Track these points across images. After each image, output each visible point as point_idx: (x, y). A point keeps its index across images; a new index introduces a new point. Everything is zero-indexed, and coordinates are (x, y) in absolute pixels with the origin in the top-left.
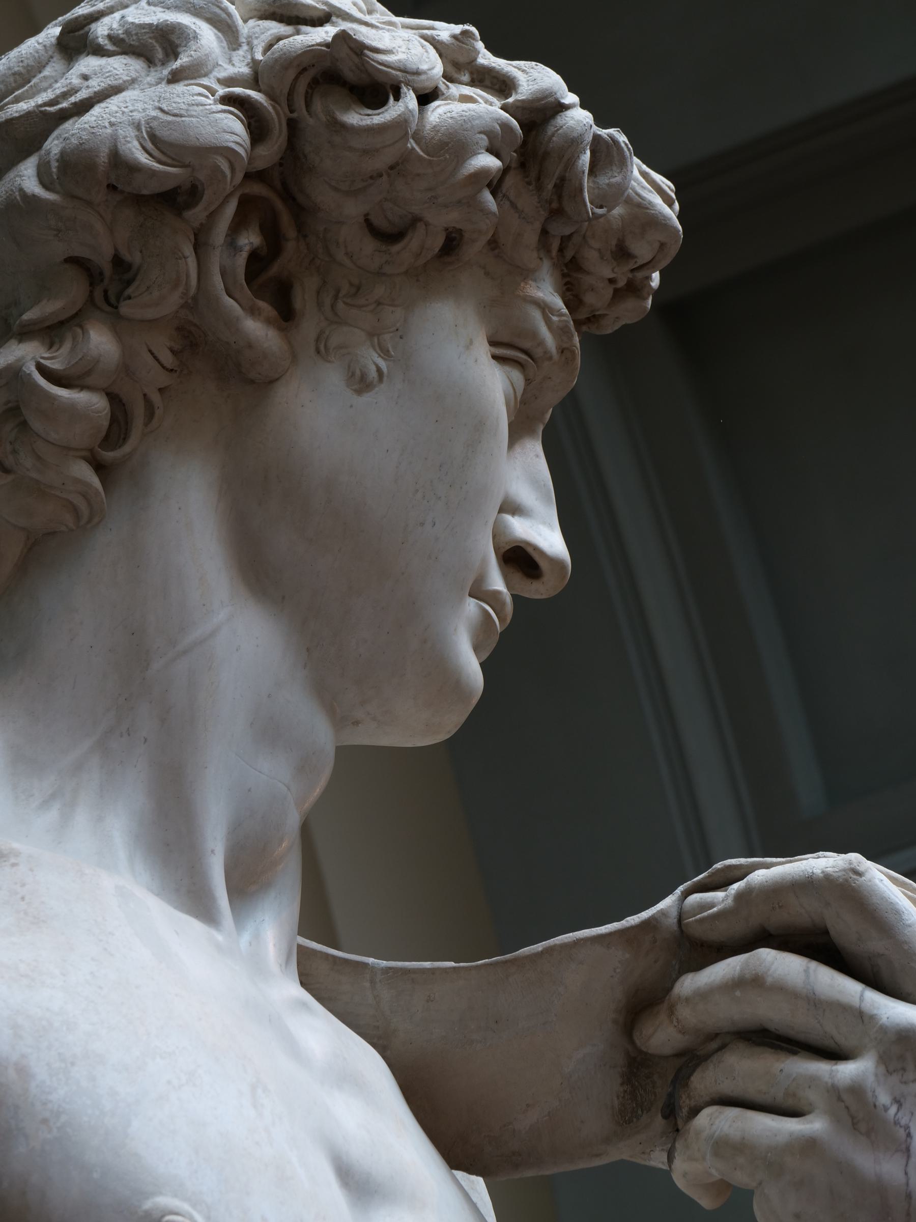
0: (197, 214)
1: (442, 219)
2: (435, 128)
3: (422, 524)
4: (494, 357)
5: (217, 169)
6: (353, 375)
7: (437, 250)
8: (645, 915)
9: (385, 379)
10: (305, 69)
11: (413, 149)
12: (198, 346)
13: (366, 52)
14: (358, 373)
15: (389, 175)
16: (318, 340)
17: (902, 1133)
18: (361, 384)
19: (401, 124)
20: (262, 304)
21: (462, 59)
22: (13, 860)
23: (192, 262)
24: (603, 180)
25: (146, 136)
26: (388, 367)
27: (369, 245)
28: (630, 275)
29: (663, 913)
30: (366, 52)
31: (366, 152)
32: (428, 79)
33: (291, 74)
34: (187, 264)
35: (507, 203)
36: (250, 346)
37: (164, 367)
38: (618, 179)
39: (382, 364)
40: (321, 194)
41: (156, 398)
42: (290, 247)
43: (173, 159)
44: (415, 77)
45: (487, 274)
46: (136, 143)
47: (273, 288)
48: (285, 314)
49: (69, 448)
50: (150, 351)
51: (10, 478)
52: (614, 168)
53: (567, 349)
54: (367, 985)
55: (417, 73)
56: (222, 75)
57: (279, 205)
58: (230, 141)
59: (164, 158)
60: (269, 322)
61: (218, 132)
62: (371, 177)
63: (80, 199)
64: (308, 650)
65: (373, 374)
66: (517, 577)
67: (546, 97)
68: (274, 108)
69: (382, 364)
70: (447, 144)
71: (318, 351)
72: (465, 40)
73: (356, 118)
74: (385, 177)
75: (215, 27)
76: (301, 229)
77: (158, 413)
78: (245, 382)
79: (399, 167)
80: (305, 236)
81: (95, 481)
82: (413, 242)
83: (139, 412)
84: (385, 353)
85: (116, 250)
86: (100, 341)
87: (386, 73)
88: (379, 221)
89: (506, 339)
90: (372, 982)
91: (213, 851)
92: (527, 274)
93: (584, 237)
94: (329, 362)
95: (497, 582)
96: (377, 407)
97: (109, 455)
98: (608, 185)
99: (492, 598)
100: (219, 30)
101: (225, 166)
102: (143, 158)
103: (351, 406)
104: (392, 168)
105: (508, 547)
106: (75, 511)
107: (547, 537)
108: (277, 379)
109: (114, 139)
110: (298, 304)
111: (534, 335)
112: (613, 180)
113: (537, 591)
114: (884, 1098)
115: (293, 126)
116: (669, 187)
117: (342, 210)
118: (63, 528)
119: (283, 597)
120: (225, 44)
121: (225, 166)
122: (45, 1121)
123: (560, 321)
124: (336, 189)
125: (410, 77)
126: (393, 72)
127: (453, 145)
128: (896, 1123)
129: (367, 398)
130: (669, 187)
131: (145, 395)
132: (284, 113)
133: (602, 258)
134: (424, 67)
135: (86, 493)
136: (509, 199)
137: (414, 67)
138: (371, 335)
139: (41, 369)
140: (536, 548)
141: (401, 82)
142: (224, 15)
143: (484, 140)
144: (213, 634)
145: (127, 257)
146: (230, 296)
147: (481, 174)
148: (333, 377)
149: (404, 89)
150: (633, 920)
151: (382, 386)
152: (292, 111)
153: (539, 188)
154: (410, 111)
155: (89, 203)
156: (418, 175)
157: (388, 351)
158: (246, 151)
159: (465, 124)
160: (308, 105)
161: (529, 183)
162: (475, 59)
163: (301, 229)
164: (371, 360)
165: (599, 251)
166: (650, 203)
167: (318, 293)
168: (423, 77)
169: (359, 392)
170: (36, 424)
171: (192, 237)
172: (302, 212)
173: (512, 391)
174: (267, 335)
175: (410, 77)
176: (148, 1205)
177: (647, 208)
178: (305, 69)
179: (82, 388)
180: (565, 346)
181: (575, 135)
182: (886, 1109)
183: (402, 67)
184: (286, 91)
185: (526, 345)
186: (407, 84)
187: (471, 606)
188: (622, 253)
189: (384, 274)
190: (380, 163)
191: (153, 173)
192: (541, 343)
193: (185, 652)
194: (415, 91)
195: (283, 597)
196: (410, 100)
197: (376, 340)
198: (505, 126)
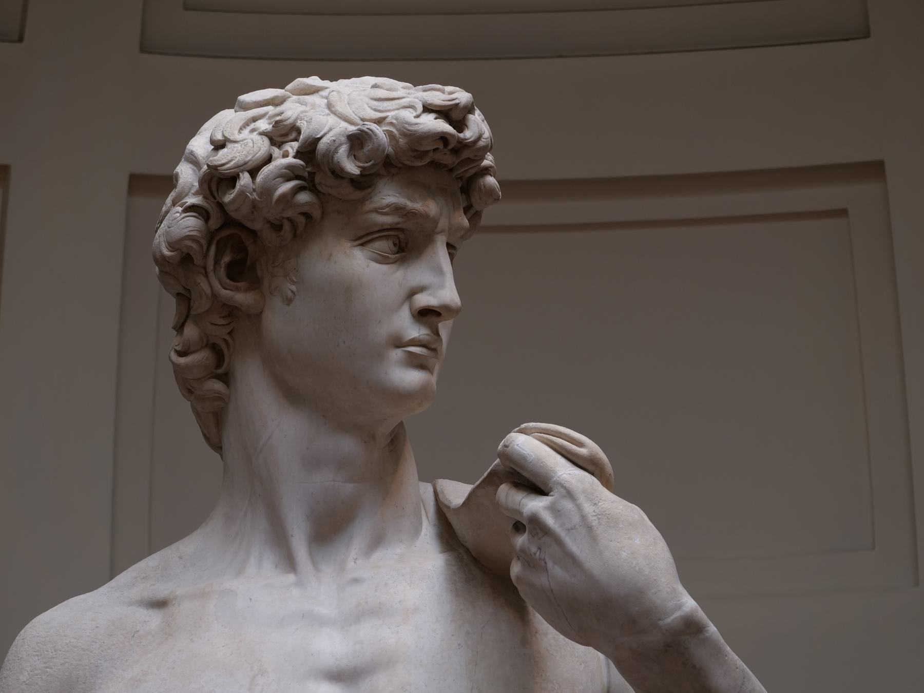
0: (198, 261)
4: (362, 245)
7: (304, 221)
12: (231, 312)
17: (543, 562)
18: (288, 301)
19: (242, 193)
20: (240, 284)
33: (206, 186)
39: (294, 288)
41: (228, 338)
42: (251, 249)
55: (246, 163)
56: (192, 191)
58: (186, 232)
65: (290, 294)
66: (433, 319)
69: (294, 288)
73: (228, 198)
77: (231, 342)
79: (254, 206)
81: (218, 386)
82: (287, 226)
83: (223, 346)
84: (293, 282)
86: (190, 331)
89: (363, 233)
95: (415, 331)
97: (220, 371)
99: (414, 342)
101: (189, 243)
102: (166, 252)
104: (254, 207)
107: (445, 292)
110: (259, 274)
114: (534, 549)
121: (189, 243)
127: (266, 191)
128: (540, 559)
138: (285, 276)
146: (225, 289)
150: (486, 474)
159: (266, 179)
169: (288, 305)
182: (535, 554)
184: (208, 192)
185: (377, 229)
186: (242, 171)
187: (397, 354)
188: (421, 155)
191: (170, 257)
192: (383, 224)
198: (290, 167)
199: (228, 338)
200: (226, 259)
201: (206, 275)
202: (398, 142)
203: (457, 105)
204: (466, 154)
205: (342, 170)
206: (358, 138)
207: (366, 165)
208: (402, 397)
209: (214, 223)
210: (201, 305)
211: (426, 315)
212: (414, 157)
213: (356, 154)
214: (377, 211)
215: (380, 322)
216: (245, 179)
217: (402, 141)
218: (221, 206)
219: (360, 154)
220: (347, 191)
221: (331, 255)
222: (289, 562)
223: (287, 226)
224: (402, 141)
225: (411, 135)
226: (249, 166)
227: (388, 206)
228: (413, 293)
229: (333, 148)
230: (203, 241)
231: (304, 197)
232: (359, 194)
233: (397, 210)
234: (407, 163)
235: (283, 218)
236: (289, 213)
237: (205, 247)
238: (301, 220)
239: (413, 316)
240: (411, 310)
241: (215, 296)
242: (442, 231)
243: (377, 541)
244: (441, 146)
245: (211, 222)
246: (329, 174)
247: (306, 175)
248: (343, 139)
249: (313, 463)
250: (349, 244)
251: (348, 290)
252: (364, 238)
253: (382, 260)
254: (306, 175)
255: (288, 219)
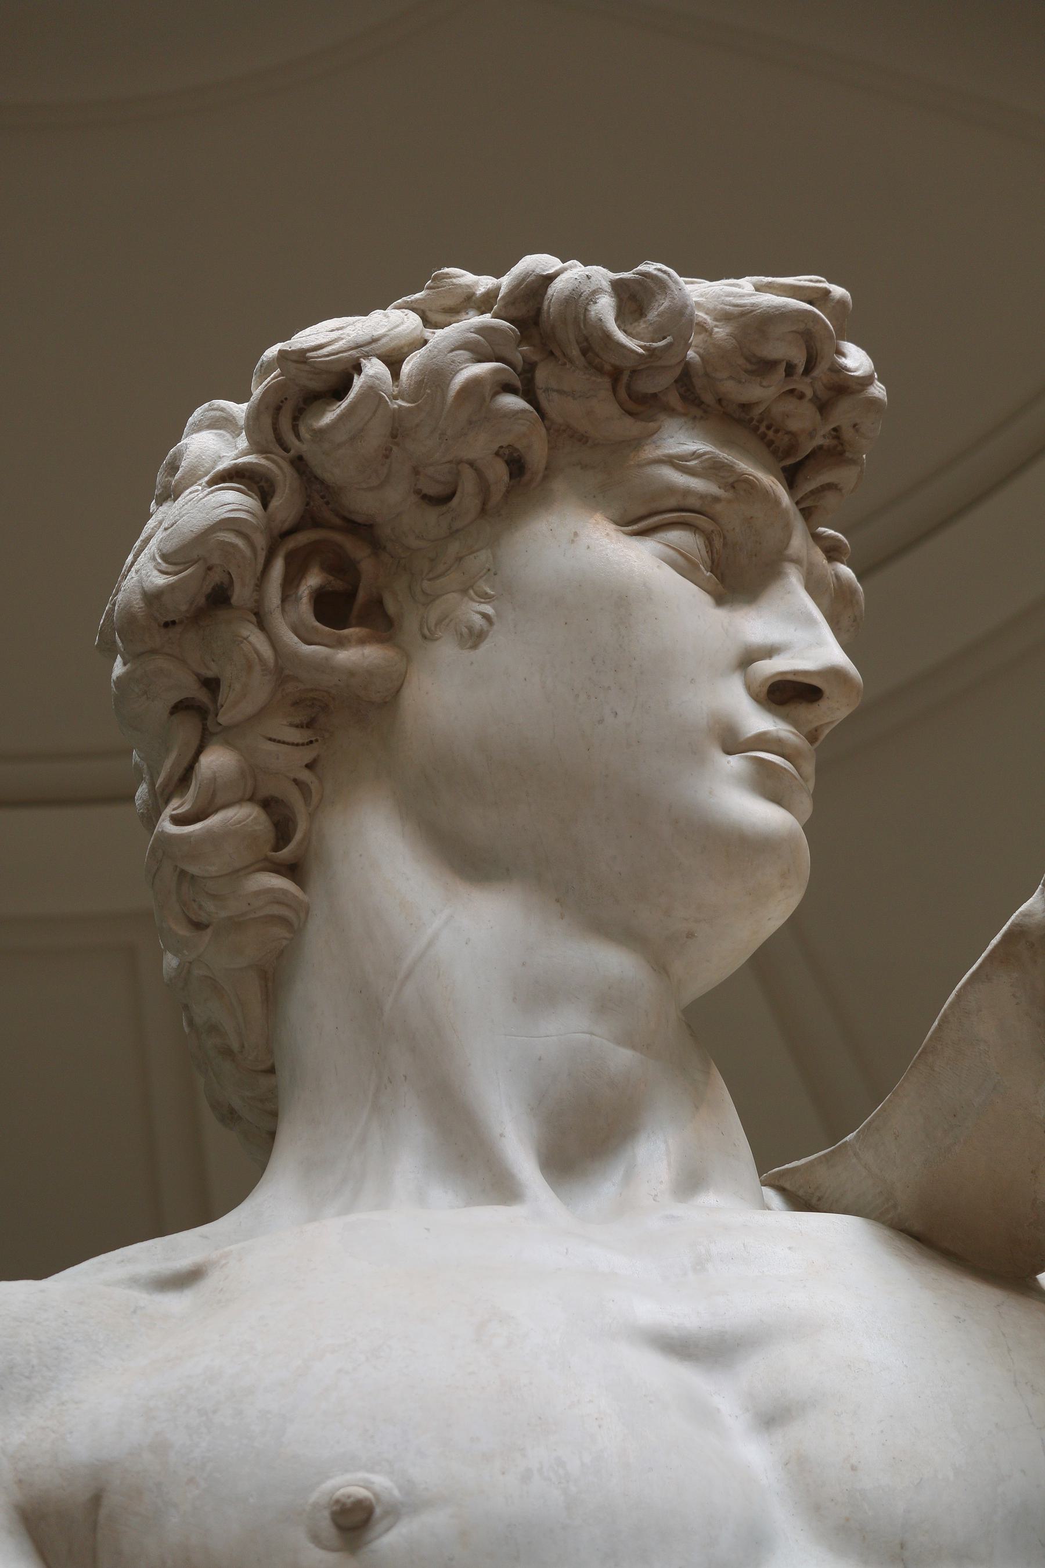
0: (241, 594)
1: (480, 446)
2: (410, 376)
3: (601, 721)
5: (223, 544)
6: (461, 634)
8: (1005, 928)
9: (495, 619)
10: (278, 409)
11: (400, 406)
13: (309, 354)
14: (465, 630)
15: (397, 444)
16: (421, 628)
18: (474, 638)
19: (371, 392)
20: (346, 632)
21: (450, 302)
22: (224, 1262)
23: (257, 640)
24: (652, 315)
25: (160, 561)
26: (494, 608)
27: (431, 515)
28: (808, 380)
29: (1024, 915)
30: (309, 354)
31: (353, 439)
32: (391, 339)
33: (267, 421)
34: (250, 643)
35: (555, 396)
36: (352, 674)
37: (297, 745)
38: (666, 303)
40: (364, 503)
41: (305, 776)
42: (367, 566)
43: (185, 563)
44: (374, 345)
45: (585, 467)
46: (156, 573)
47: (335, 610)
48: (380, 623)
49: (238, 871)
50: (270, 739)
51: (209, 931)
52: (659, 297)
53: (737, 481)
54: (854, 1160)
55: (374, 340)
57: (338, 537)
58: (223, 513)
59: (181, 567)
60: (362, 642)
61: (207, 514)
62: (387, 457)
63: (143, 653)
64: (557, 901)
65: (478, 621)
67: (523, 280)
68: (267, 458)
69: (488, 609)
70: (422, 381)
71: (425, 637)
72: (439, 284)
73: (330, 416)
74: (395, 449)
75: (212, 428)
76: (376, 545)
77: (314, 787)
78: (372, 708)
79: (398, 429)
80: (385, 548)
82: (468, 484)
83: (295, 797)
84: (486, 598)
85: (198, 675)
86: (216, 761)
87: (338, 360)
88: (433, 490)
89: (642, 511)
90: (856, 1154)
91: (501, 1135)
92: (637, 443)
93: (707, 375)
94: (437, 639)
96: (502, 650)
97: (285, 853)
98: (658, 315)
99: (762, 742)
100: (220, 429)
103: (472, 663)
104: (394, 436)
105: (765, 689)
106: (284, 921)
108: (402, 685)
109: (140, 581)
111: (671, 490)
112: (662, 308)
113: (834, 711)
115: (299, 463)
116: (811, 281)
117: (387, 501)
118: (285, 942)
119: (508, 870)
120: (228, 436)
122: (191, 1481)
123: (701, 462)
124: (370, 489)
125: (366, 349)
126: (345, 354)
127: (434, 378)
129: (485, 646)
130: (811, 281)
131: (295, 780)
132: (282, 457)
133: (740, 382)
134: (381, 331)
135: (277, 897)
136: (554, 390)
137: (367, 338)
138: (464, 592)
139: (177, 820)
140: (795, 673)
141: (358, 358)
142: (218, 413)
143: (464, 354)
144: (430, 944)
145: (210, 674)
147: (473, 385)
148: (446, 650)
149: (363, 361)
151: (495, 627)
152: (287, 450)
153: (571, 361)
154: (372, 377)
155: (153, 651)
156: (417, 425)
157: (487, 594)
158: (248, 511)
160: (298, 436)
161: (565, 364)
162: (474, 294)
163: (376, 545)
164: (474, 611)
165: (731, 378)
166: (753, 305)
167: (410, 587)
168: (384, 341)
169: (475, 646)
170: (193, 869)
171: (254, 619)
172: (363, 530)
173: (671, 552)
174: (363, 654)
175: (366, 349)
176: (314, 1497)
177: (752, 311)
178: (278, 409)
179: (216, 811)
180: (731, 480)
181: (567, 293)
183: (352, 345)
184: (271, 437)
185: (672, 502)
186: (367, 356)
188: (764, 367)
189: (457, 531)
190: (375, 438)
191: (171, 588)
192: (687, 492)
193: (407, 977)
194: (379, 357)
195: (508, 870)
196: (375, 368)
197: (471, 592)
199: (305, 776)
200: (313, 580)
201: (261, 622)
202: (709, 332)
203: (827, 292)
204: (843, 414)
205: (608, 336)
206: (633, 297)
207: (655, 345)
208: (743, 847)
209: (286, 504)
210: (245, 696)
211: (787, 694)
212: (746, 371)
213: (629, 328)
214: (674, 462)
215: (692, 681)
216: (375, 368)
217: (721, 332)
218: (299, 463)
219: (641, 326)
220: (603, 412)
221: (576, 534)
222: (502, 1188)
223: (468, 484)
224: (721, 332)
225: (743, 314)
226: (383, 345)
227: (695, 455)
228: (748, 658)
229: (587, 290)
230: (261, 541)
231: (512, 402)
232: (630, 427)
233: (714, 469)
234: (731, 389)
235: (459, 462)
236: (480, 446)
237: (261, 560)
238: (499, 472)
239: (756, 698)
240: (748, 688)
241: (284, 670)
242: (797, 561)
243: (691, 1182)
244: (799, 359)
245: (275, 503)
246: (575, 352)
247: (518, 359)
248: (606, 285)
249: (538, 994)
250: (614, 526)
251: (622, 602)
252: (641, 521)
253: (686, 567)
254: (518, 359)
255: (471, 464)
